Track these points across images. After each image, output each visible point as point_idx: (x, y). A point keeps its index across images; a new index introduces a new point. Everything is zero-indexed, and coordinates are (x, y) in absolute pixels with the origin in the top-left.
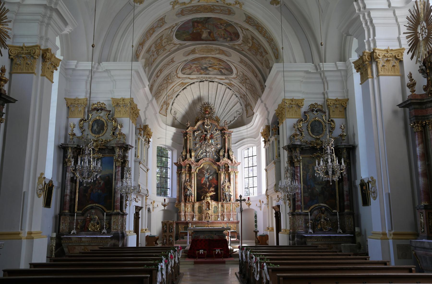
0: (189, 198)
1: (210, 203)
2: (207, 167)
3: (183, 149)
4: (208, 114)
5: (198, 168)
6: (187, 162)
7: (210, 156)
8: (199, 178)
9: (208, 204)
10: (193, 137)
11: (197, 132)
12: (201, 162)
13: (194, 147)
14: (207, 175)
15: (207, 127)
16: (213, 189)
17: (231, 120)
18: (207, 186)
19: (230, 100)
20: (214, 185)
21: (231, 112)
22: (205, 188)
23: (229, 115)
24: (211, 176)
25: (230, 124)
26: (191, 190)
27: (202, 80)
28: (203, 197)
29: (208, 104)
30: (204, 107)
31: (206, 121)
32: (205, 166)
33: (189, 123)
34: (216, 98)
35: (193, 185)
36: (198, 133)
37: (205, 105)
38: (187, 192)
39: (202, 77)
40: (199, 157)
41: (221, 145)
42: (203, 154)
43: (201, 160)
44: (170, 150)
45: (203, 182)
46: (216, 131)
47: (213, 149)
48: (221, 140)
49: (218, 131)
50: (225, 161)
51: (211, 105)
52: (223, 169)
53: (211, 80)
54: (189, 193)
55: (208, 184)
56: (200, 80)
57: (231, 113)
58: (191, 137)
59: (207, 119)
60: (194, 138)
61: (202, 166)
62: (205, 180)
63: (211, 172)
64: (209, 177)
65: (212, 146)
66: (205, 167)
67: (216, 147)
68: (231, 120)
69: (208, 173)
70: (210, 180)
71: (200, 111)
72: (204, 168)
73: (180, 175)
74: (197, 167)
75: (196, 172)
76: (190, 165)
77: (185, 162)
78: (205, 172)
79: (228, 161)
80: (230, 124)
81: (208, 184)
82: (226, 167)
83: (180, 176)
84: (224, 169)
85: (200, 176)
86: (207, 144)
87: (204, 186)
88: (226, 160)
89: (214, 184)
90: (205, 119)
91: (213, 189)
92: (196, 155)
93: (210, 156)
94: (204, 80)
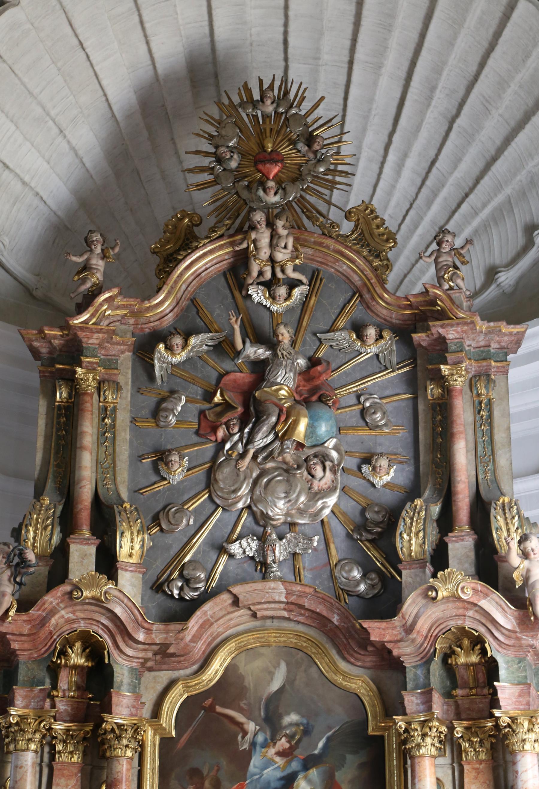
2: (271, 674)
3: (38, 494)
4: (279, 182)
5: (179, 688)
6: (65, 614)
7: (296, 572)
10: (138, 390)
11: (177, 341)
12: (206, 625)
13: (144, 482)
15: (273, 297)
17: (498, 262)
19: (482, 65)
21: (498, 188)
23: (476, 213)
24: (314, 773)
25: (492, 292)
29: (277, 102)
30: (239, 125)
33: (104, 256)
34: (351, 63)
36: (180, 357)
37: (255, 104)
40: (187, 581)
41: (409, 469)
42: (235, 548)
43: (208, 608)
46: (361, 337)
47: (332, 501)
48: (406, 420)
49: (371, 332)
50: (451, 609)
51: (306, 106)
52: (437, 698)
57: (500, 198)
58: (118, 388)
59: (270, 224)
60: (151, 400)
63: (307, 731)
65: (318, 471)
66: (249, 681)
67: (355, 482)
68: (498, 259)
69: (283, 743)
71: (206, 161)
72: (242, 691)
74: (164, 677)
75: (158, 729)
77: (43, 621)
78: (251, 727)
79: (484, 603)
80: (492, 292)
82: (461, 673)
84: (448, 695)
86: (270, 456)
88: (467, 595)
90: (253, 228)
92: (159, 565)
93: (296, 572)
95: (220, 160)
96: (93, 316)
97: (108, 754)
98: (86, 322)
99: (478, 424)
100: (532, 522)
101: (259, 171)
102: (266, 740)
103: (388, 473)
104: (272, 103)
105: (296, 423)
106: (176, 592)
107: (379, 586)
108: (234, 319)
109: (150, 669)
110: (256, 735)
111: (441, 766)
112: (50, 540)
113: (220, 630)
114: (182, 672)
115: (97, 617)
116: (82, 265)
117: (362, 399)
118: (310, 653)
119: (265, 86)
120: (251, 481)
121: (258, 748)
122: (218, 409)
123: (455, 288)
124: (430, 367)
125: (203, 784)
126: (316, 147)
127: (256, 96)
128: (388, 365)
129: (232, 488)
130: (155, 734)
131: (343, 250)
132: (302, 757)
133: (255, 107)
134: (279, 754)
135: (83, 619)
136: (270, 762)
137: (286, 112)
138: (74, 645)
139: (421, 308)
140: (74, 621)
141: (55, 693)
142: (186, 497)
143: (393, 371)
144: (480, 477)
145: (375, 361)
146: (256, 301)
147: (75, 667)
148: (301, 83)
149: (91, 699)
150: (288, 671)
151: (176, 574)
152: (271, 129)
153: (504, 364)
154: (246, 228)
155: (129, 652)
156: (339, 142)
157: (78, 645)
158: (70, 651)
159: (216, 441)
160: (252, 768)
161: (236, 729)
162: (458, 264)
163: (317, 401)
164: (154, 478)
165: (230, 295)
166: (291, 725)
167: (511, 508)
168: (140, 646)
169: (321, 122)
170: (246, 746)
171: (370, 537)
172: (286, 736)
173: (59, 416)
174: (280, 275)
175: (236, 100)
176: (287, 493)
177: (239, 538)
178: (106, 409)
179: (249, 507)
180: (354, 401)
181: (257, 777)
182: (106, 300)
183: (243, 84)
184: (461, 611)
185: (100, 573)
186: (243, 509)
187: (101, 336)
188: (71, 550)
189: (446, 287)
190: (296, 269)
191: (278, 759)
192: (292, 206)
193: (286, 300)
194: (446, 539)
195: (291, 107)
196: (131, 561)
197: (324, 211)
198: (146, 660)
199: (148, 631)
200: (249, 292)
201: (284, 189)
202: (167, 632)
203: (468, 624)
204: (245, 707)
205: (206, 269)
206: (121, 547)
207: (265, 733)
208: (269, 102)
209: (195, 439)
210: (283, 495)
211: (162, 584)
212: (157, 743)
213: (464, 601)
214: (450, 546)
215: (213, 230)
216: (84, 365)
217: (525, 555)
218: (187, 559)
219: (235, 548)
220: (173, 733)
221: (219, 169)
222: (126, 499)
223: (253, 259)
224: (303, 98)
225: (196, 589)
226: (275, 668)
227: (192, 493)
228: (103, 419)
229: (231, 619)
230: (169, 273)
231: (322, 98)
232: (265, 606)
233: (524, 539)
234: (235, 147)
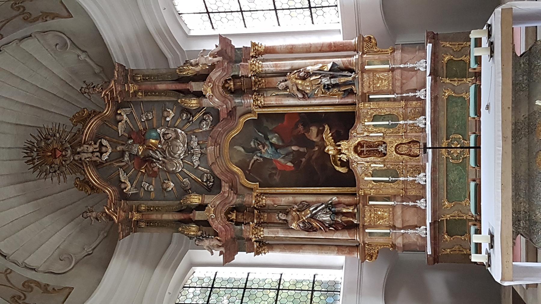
0: (344, 214)
1: (359, 140)
8: (277, 178)
9: (362, 146)
14: (267, 152)
16: (314, 130)
18: (302, 150)
20: (301, 128)
22: (310, 158)
24: (270, 137)
26: (316, 205)
28: (337, 168)
30: (41, 165)
31: (86, 155)
32: (237, 159)
35: (300, 199)
36: (129, 184)
38: (322, 223)
40: (207, 180)
42: (196, 164)
44: (191, 272)
45: (289, 164)
49: (118, 117)
51: (33, 140)
54: (327, 213)
55: (294, 148)
59: (79, 153)
61: (236, 169)
62: (283, 158)
63: (257, 139)
64: (271, 144)
66: (241, 158)
69: (260, 147)
70: (283, 141)
73: (264, 244)
76: (232, 210)
78: (255, 157)
81: (294, 148)
83: (270, 242)
85: (271, 175)
87: (304, 160)
89: (296, 127)
90: (80, 159)
91: (314, 130)
96: (114, 215)
97: (264, 204)
98: (116, 217)
99: (151, 80)
100: (185, 62)
101: (59, 157)
102: (259, 153)
103: (169, 111)
104: (33, 153)
105: (152, 143)
106: (211, 184)
107: (208, 115)
108: (114, 165)
109: (237, 191)
110: (257, 156)
111: (267, 94)
112: (194, 227)
113: (224, 168)
114: (238, 181)
115: (219, 210)
116: (95, 219)
117: (143, 120)
118: (231, 138)
119: (27, 155)
120: (173, 159)
121: (262, 155)
122: (147, 171)
123: (102, 87)
124: (131, 97)
125: (274, 173)
126: (49, 137)
127: (30, 158)
128: (130, 111)
129: (175, 164)
130: (257, 189)
131: (88, 127)
132: (265, 140)
133: (34, 159)
134: (264, 148)
135: (221, 214)
136: (266, 151)
137: (36, 147)
138: (229, 217)
139: (109, 99)
140: (221, 217)
141: (245, 223)
142: (178, 181)
143: (133, 109)
144: (170, 80)
145: (129, 116)
146: (108, 158)
147: (236, 216)
148: (25, 142)
149: (247, 211)
150: (238, 145)
151: (205, 184)
152: (43, 153)
153: (129, 70)
154: (81, 162)
155: (231, 198)
156: (47, 129)
157: (229, 216)
158: (231, 219)
159: (159, 171)
160: (268, 157)
162: (93, 86)
163: (144, 136)
164: (172, 192)
165: (106, 167)
166: (255, 145)
167: (181, 69)
168: (230, 195)
169: (40, 135)
170: (261, 159)
171: (191, 118)
172: (258, 146)
173: (151, 226)
174: (98, 150)
175: (32, 166)
177: (192, 162)
178: (147, 210)
179: (182, 159)
180: (143, 123)
181: (271, 155)
182: (108, 211)
183: (25, 163)
184: (216, 87)
185: (205, 209)
186: (182, 162)
187: (121, 212)
188: (197, 219)
189: (101, 90)
190: (95, 144)
191: (265, 149)
192: (72, 145)
193: (107, 147)
194: (192, 92)
195: (34, 146)
196: (201, 199)
197: (73, 134)
198: (234, 193)
199: (224, 192)
200: (104, 160)
201: (66, 148)
202: (225, 186)
203: (221, 85)
204: (249, 160)
205: (96, 175)
206: (196, 203)
207: (257, 153)
208: (32, 154)
209: (158, 178)
210: (177, 147)
211: (209, 188)
212: (260, 188)
213: (213, 85)
214: (194, 90)
215: (81, 174)
216: (132, 217)
217: (197, 65)
218: (200, 180)
220: (258, 183)
221: (58, 172)
222: (179, 202)
223: (92, 159)
224: (31, 141)
225: (210, 177)
226: (236, 150)
227: (177, 179)
228: (151, 210)
229: (220, 165)
230: (98, 188)
231: (30, 134)
232: (216, 153)
233: (191, 65)
234: (50, 166)
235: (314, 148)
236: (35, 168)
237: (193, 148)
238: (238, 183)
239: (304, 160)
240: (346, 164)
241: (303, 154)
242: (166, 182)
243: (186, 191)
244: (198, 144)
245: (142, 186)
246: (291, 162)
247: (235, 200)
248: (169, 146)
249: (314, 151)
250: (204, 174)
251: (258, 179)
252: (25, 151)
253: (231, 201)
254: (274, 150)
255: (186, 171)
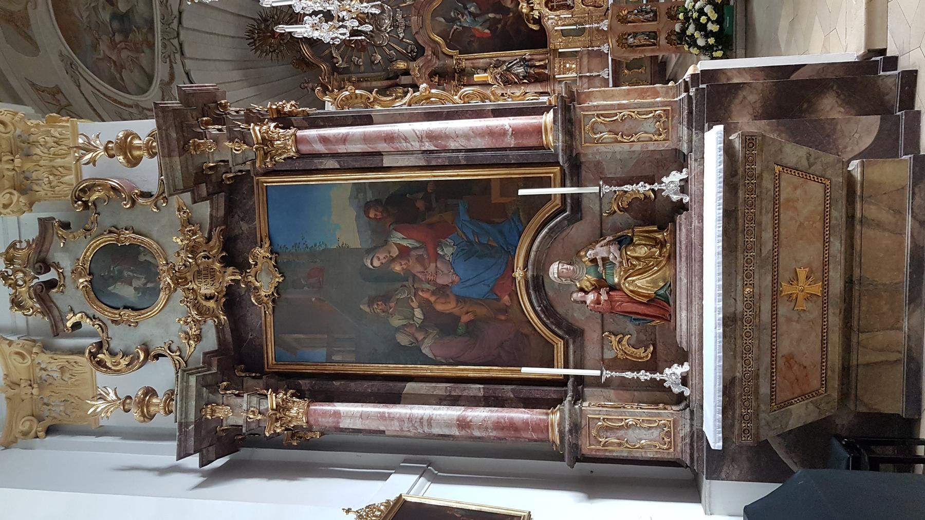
2: (440, 22)
8: (475, 45)
11: (335, 61)
14: (466, 21)
18: (498, 16)
24: (468, 6)
27: (178, 47)
30: (261, 45)
36: (340, 58)
38: (517, 75)
39: (165, 46)
40: (412, 51)
42: (401, 36)
45: (487, 31)
53: (176, 22)
55: (491, 15)
56: (178, 56)
61: (438, 39)
62: (481, 25)
63: (456, 9)
64: (470, 13)
70: (480, 9)
78: (455, 27)
81: (491, 15)
85: (470, 43)
87: (499, 26)
94: (175, 42)
95: (274, 51)
127: (252, 40)
133: (255, 40)
134: (463, 17)
147: (439, 80)
161: (456, 32)
176: (383, 19)
195: (255, 28)
199: (428, 56)
209: (366, 52)
219: (401, 36)
224: (252, 25)
235: (509, 14)
236: (257, 49)
237: (397, 21)
238: (440, 52)
239: (499, 26)
240: (538, 21)
241: (499, 21)
242: (374, 54)
243: (391, 61)
244: (403, 17)
245: (352, 61)
246: (488, 29)
247: (437, 64)
248: (376, 21)
249: (509, 18)
250: (408, 46)
251: (458, 47)
252: (248, 34)
253: (434, 65)
254: (472, 18)
255: (392, 44)
